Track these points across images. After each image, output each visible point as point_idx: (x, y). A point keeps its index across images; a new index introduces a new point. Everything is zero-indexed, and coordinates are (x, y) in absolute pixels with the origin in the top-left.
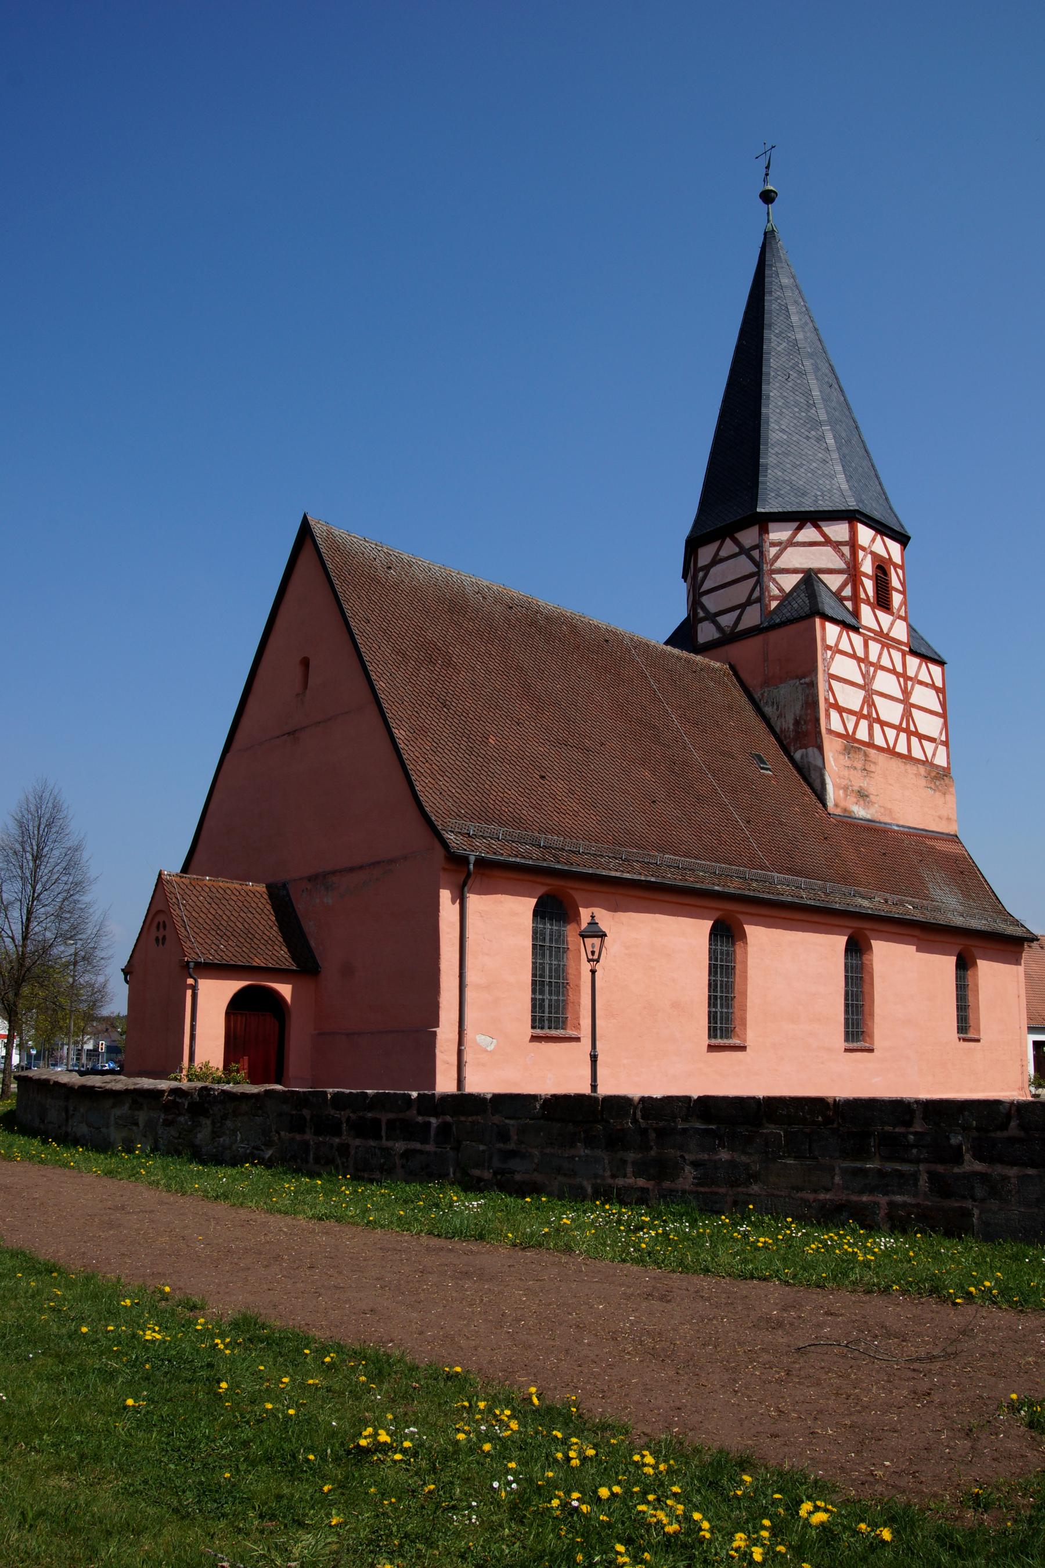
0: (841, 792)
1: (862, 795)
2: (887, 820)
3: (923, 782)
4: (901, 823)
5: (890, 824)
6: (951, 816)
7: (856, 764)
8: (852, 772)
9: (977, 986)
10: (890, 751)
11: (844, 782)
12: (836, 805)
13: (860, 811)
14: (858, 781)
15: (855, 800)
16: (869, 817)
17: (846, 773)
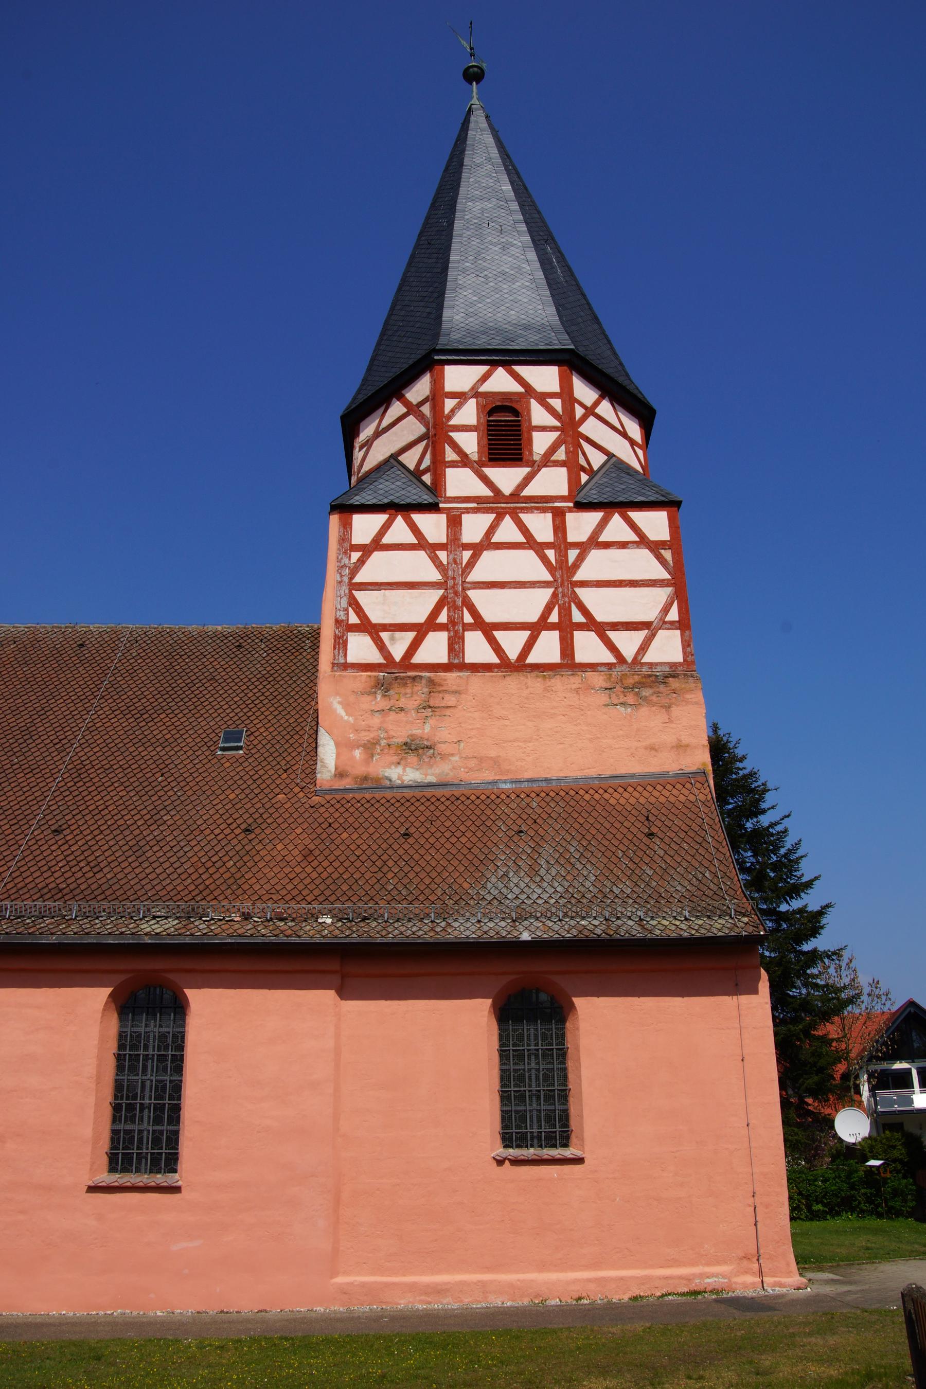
0: (357, 753)
1: (414, 748)
2: (488, 776)
3: (603, 698)
4: (527, 775)
5: (495, 782)
6: (686, 740)
7: (402, 702)
8: (392, 716)
9: (577, 1049)
10: (505, 666)
11: (366, 736)
12: (340, 774)
13: (405, 774)
14: (403, 728)
15: (395, 759)
16: (431, 779)
17: (376, 720)
